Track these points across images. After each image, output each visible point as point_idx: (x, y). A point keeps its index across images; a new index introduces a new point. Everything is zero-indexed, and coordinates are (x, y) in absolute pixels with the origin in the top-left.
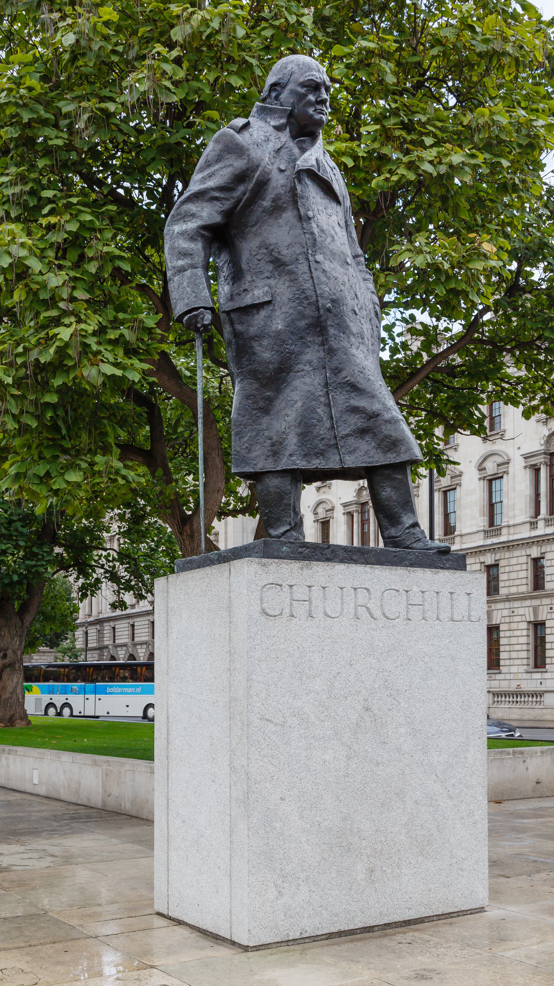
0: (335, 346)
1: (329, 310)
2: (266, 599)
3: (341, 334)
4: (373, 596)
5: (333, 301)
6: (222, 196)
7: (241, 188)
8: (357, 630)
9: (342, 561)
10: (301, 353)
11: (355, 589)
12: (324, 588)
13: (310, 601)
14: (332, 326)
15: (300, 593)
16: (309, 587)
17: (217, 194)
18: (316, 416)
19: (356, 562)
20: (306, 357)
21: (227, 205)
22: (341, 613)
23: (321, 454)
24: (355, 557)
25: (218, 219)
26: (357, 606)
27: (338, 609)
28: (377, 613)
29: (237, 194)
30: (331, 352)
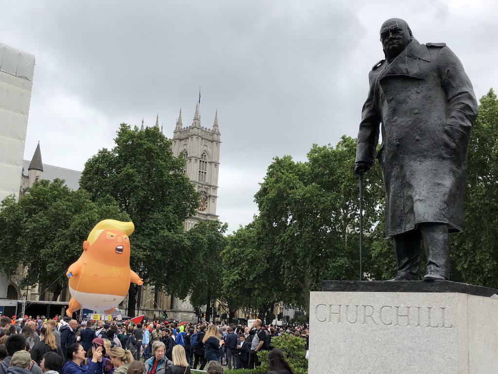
0: (403, 164)
1: (398, 145)
2: (318, 312)
3: (406, 156)
4: (375, 310)
5: (399, 140)
6: (370, 103)
7: (374, 97)
8: (365, 330)
9: (362, 290)
10: (391, 172)
11: (365, 306)
12: (348, 306)
13: (339, 313)
14: (401, 153)
15: (335, 309)
16: (340, 306)
17: (368, 104)
18: (397, 205)
19: (370, 290)
20: (393, 174)
21: (372, 106)
22: (356, 320)
23: (399, 225)
24: (369, 288)
25: (369, 115)
26: (365, 316)
27: (354, 318)
28: (378, 321)
29: (373, 100)
30: (402, 167)
